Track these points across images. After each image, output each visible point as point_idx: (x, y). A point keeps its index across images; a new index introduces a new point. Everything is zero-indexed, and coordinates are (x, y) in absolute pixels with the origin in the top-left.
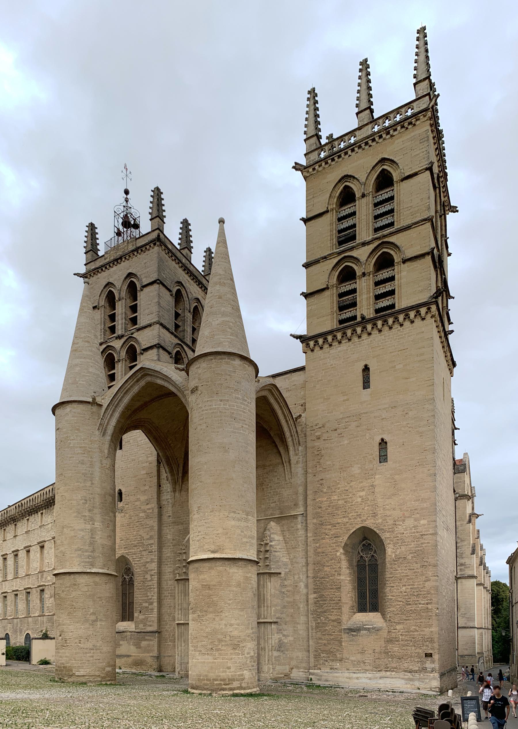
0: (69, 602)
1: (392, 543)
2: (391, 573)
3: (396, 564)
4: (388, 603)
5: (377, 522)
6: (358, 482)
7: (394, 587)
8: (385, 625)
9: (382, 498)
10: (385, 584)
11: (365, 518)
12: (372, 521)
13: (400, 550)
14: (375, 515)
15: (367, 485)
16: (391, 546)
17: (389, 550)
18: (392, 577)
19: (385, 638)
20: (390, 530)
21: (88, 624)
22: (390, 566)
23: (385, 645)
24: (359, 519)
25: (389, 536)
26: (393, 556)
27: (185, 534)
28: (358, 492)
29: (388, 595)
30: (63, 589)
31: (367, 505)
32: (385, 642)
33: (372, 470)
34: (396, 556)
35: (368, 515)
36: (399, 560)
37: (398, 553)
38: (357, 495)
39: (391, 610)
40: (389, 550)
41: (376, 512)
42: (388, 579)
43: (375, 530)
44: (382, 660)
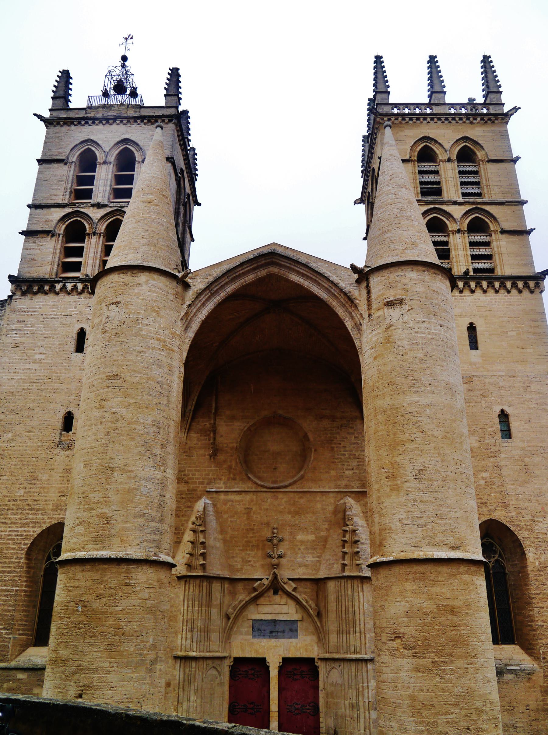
0: (111, 622)
1: (533, 545)
2: (537, 588)
3: (541, 575)
4: (538, 632)
5: (510, 514)
6: (478, 459)
7: (543, 608)
8: (536, 665)
9: (512, 484)
10: (529, 603)
11: (493, 508)
12: (503, 512)
13: (545, 555)
14: (505, 505)
15: (490, 464)
16: (532, 549)
17: (530, 554)
18: (539, 594)
19: (541, 686)
20: (529, 527)
21: (143, 669)
22: (535, 578)
23: (543, 697)
24: (484, 508)
25: (527, 536)
26: (537, 564)
27: (191, 500)
28: (479, 472)
29: (537, 619)
30: (101, 591)
31: (493, 490)
32: (541, 692)
33: (494, 445)
34: (540, 564)
35: (497, 504)
36: (545, 570)
37: (542, 560)
38: (479, 476)
39: (543, 642)
40: (531, 555)
41: (506, 501)
42: (534, 596)
43: (508, 525)
44: (542, 722)
